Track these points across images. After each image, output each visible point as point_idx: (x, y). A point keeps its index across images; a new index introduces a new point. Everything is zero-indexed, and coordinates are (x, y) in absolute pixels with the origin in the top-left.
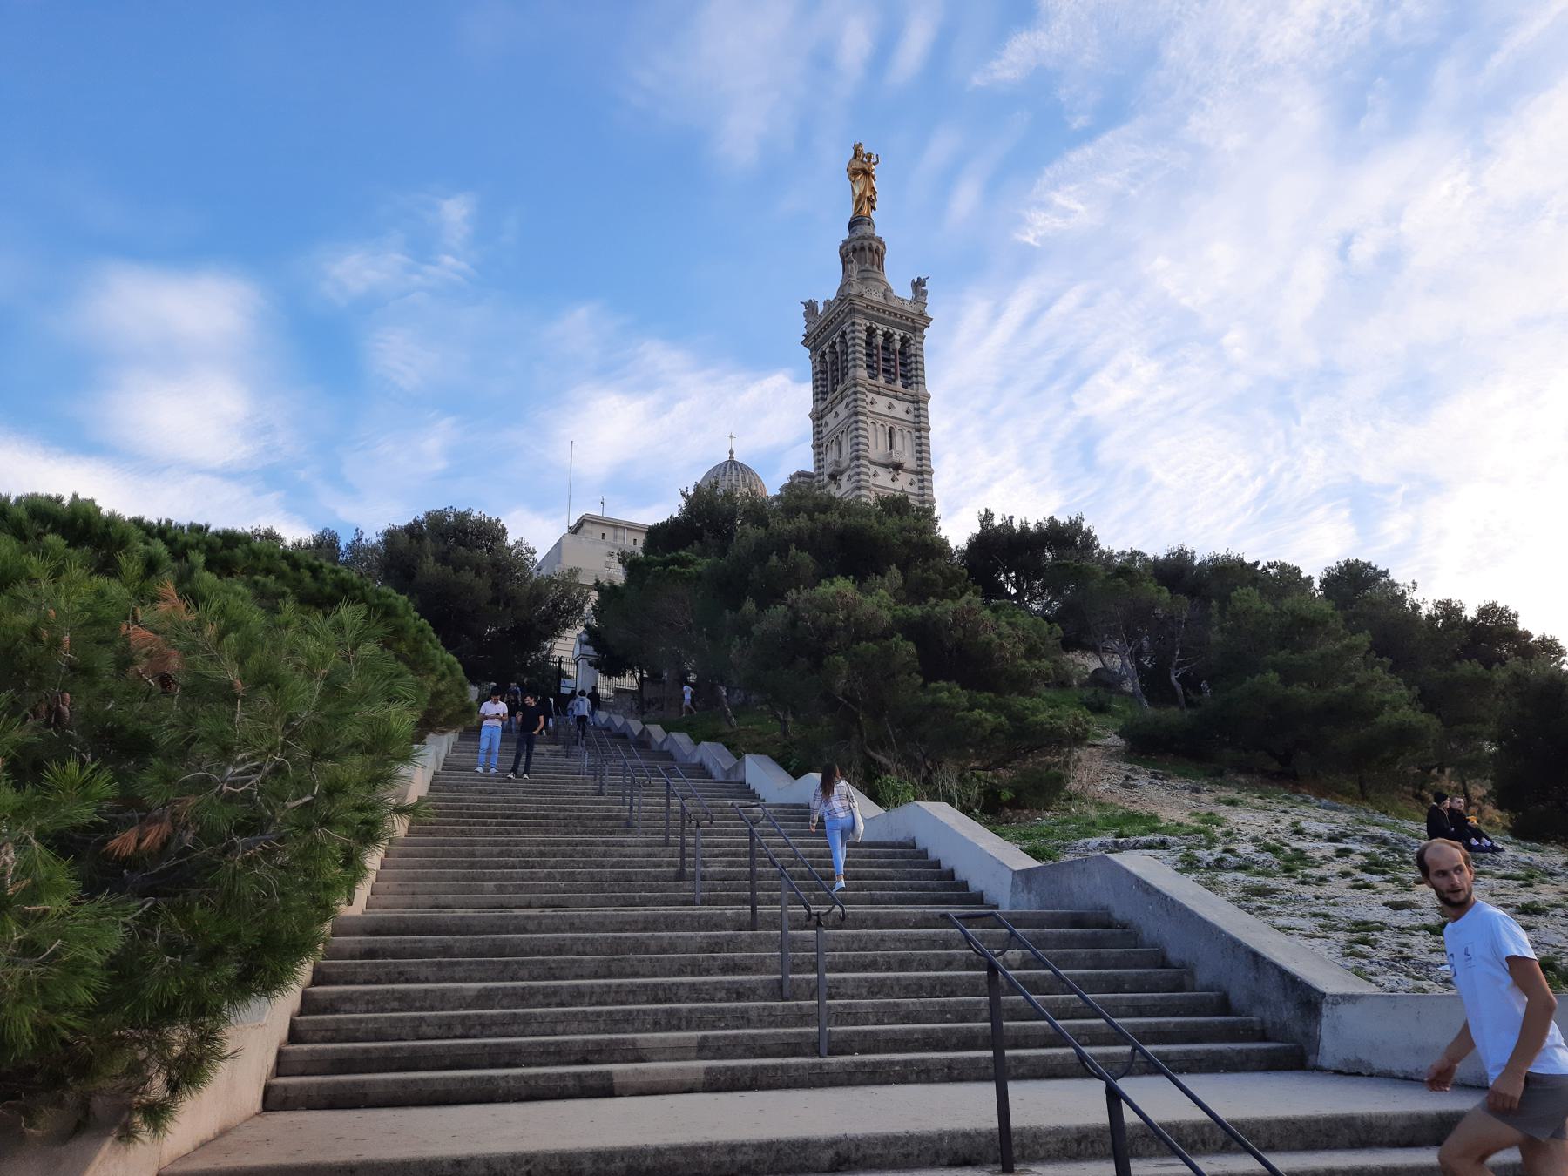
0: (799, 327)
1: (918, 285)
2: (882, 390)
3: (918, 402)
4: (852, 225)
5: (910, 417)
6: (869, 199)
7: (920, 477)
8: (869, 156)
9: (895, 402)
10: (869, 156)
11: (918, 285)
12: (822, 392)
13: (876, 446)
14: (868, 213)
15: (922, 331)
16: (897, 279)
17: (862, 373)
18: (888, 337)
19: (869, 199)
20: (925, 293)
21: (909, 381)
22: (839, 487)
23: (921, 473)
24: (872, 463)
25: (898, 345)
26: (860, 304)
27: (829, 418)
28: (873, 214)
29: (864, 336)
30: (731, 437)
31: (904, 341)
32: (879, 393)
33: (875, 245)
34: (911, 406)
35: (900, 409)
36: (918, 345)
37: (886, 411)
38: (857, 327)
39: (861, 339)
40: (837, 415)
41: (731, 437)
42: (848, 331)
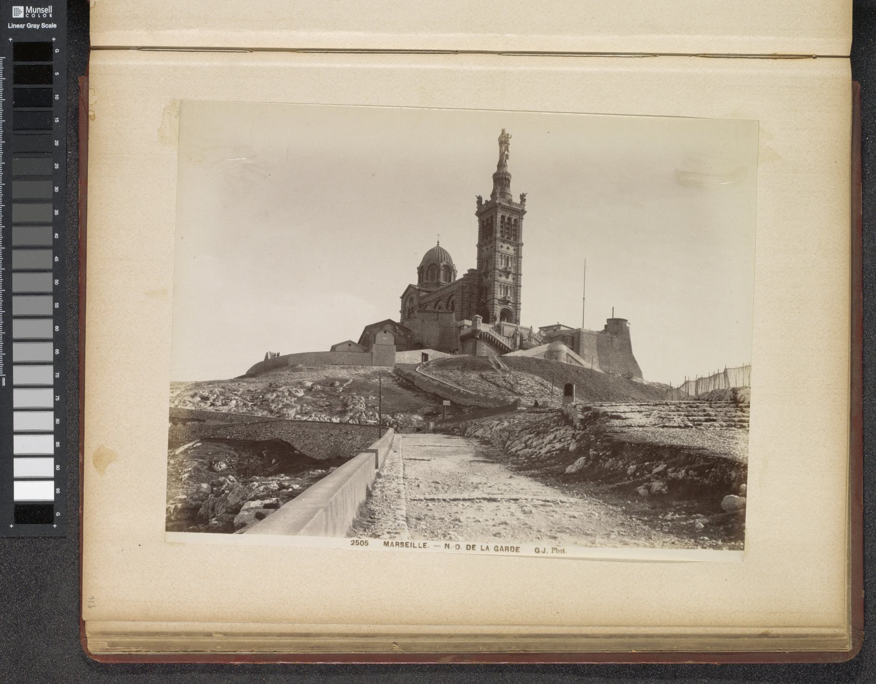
0: (474, 208)
1: (523, 197)
8: (508, 135)
10: (508, 135)
11: (523, 197)
13: (501, 266)
14: (506, 161)
16: (515, 192)
18: (509, 219)
20: (525, 200)
22: (486, 278)
27: (485, 248)
28: (507, 161)
30: (438, 235)
31: (515, 220)
33: (507, 177)
40: (487, 249)
41: (438, 235)
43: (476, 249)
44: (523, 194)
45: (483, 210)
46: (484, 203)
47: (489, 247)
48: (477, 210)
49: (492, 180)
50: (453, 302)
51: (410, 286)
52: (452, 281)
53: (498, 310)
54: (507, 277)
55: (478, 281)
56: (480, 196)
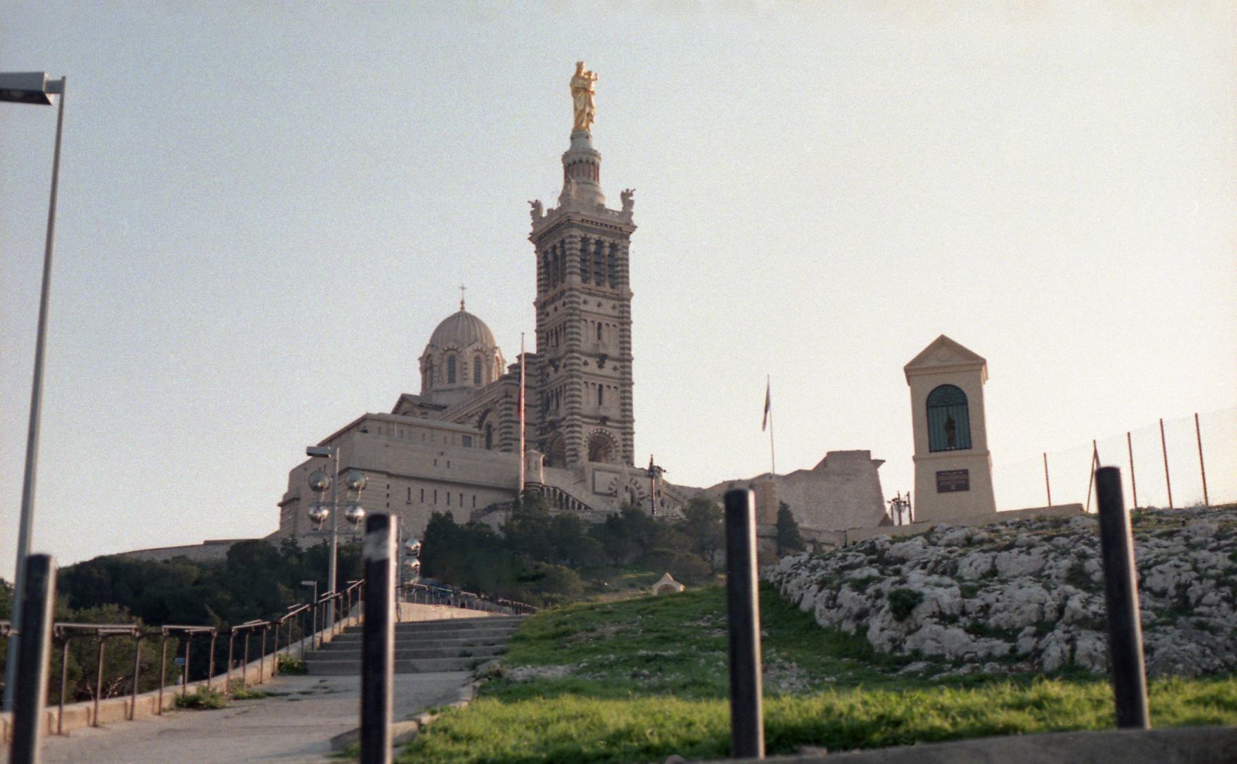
0: (526, 226)
1: (626, 197)
2: (593, 291)
3: (623, 300)
4: (572, 138)
5: (616, 313)
6: (588, 114)
7: (622, 364)
8: (589, 73)
9: (603, 301)
11: (626, 197)
12: (545, 285)
13: (586, 339)
14: (587, 127)
15: (627, 238)
17: (576, 280)
18: (599, 243)
19: (589, 114)
20: (632, 203)
21: (616, 281)
22: (556, 370)
23: (623, 360)
24: (581, 353)
25: (607, 251)
26: (577, 219)
27: (550, 309)
28: (591, 125)
29: (579, 246)
30: (463, 288)
31: (613, 247)
32: (590, 294)
34: (617, 303)
35: (607, 307)
36: (625, 250)
37: (595, 309)
38: (575, 240)
39: (576, 249)
40: (556, 309)
41: (463, 288)
42: (567, 241)
43: (533, 311)
44: (627, 190)
45: (544, 227)
46: (544, 214)
47: (559, 304)
48: (531, 229)
49: (562, 165)
50: (489, 426)
51: (404, 399)
52: (484, 383)
53: (584, 439)
54: (601, 366)
55: (539, 378)
56: (537, 201)
